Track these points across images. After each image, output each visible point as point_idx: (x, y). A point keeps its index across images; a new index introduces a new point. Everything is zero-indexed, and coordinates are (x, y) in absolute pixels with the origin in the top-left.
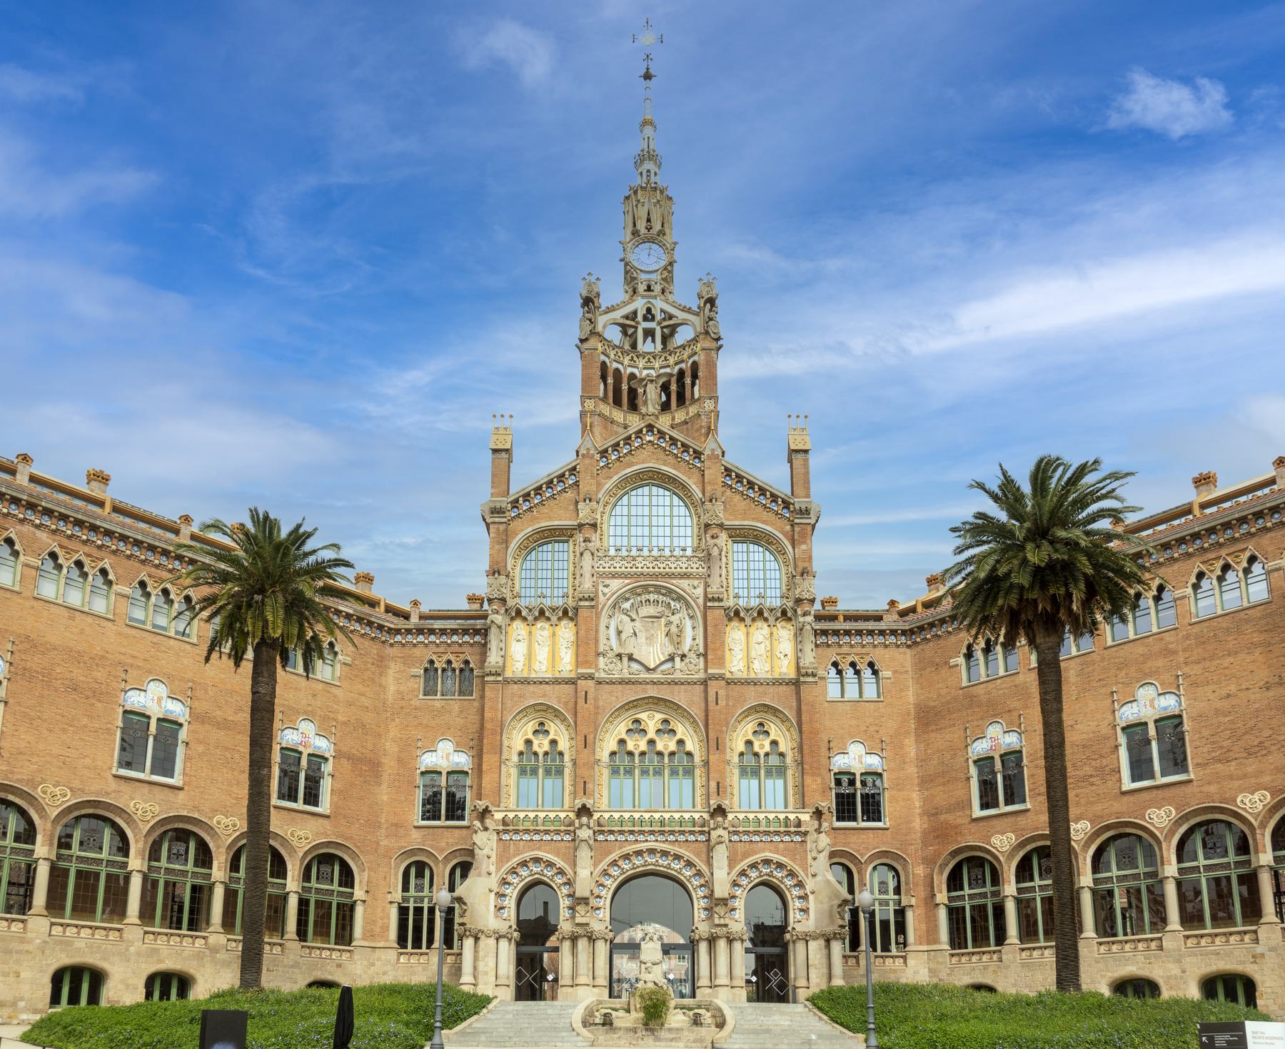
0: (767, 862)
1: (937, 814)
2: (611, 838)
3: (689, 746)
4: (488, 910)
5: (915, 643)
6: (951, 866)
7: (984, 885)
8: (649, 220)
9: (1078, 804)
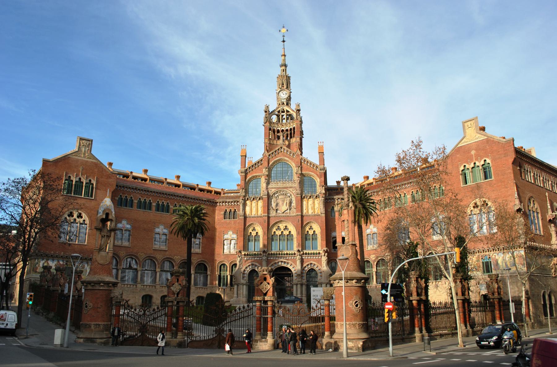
0: (311, 264)
2: (272, 258)
3: (292, 233)
4: (241, 277)
8: (283, 84)
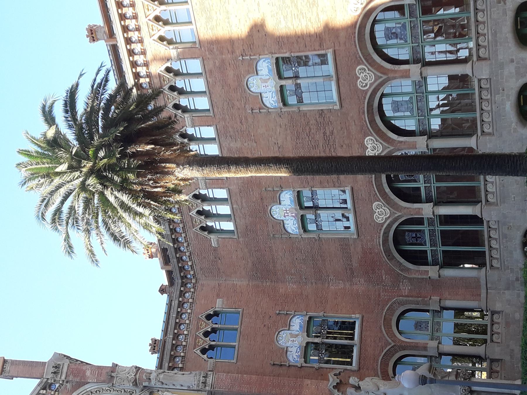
1: (351, 269)
5: (194, 276)
6: (402, 261)
7: (422, 232)
9: (349, 146)
